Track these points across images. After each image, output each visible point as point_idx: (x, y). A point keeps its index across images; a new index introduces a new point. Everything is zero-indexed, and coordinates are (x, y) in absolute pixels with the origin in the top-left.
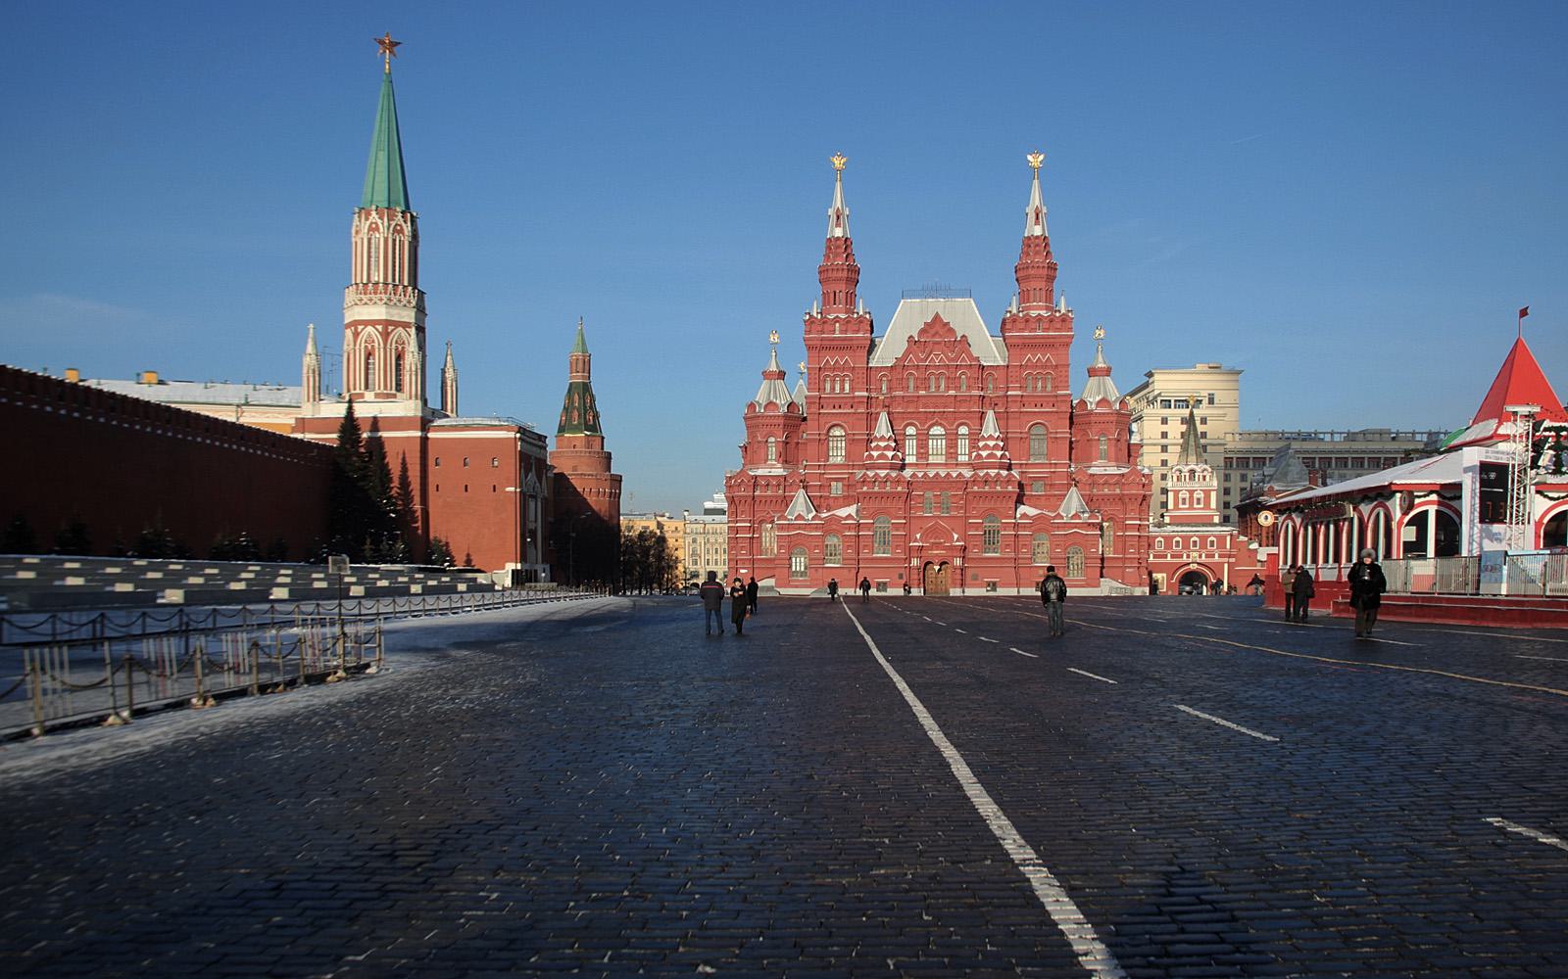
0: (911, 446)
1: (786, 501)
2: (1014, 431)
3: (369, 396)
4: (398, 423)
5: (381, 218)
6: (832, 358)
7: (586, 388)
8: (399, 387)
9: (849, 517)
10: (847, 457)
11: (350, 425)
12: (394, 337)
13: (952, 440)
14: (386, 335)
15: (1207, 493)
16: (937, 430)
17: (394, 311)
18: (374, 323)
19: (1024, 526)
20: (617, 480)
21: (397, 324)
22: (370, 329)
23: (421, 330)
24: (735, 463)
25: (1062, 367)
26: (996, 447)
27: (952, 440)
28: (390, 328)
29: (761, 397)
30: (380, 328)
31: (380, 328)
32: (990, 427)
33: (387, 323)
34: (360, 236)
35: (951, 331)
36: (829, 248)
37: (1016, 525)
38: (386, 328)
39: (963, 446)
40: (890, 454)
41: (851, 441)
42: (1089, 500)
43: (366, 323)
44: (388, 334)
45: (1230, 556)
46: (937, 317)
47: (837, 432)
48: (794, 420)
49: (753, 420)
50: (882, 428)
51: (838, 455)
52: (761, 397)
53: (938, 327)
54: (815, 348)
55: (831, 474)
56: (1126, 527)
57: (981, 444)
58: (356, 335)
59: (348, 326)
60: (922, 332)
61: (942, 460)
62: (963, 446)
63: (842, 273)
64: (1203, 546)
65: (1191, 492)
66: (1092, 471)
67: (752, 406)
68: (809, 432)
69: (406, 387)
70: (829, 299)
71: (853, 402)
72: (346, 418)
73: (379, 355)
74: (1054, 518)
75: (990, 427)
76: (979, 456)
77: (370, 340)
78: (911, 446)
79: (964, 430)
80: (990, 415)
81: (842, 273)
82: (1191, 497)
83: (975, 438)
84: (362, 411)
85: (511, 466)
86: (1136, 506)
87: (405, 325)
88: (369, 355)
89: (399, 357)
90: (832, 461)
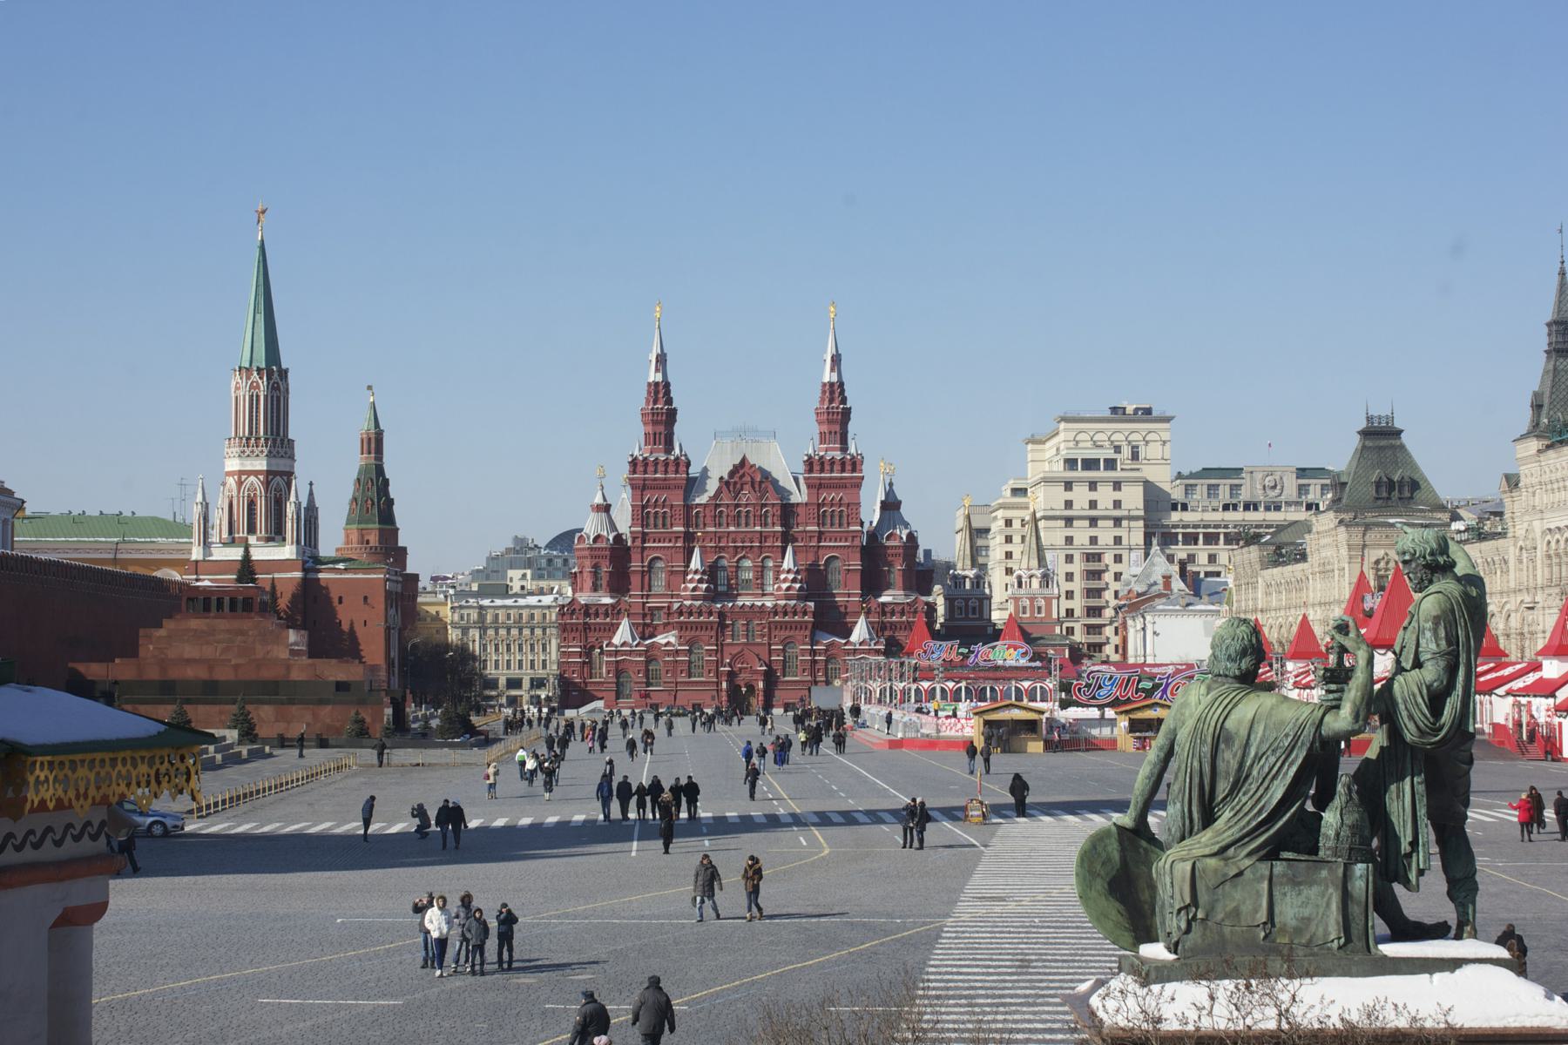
1: (613, 628)
7: (380, 470)
9: (668, 644)
10: (668, 586)
11: (247, 568)
13: (761, 571)
15: (1048, 600)
16: (748, 563)
17: (274, 461)
18: (256, 473)
22: (252, 478)
32: (788, 562)
43: (249, 473)
46: (744, 461)
48: (619, 552)
50: (695, 563)
53: (746, 469)
54: (639, 488)
55: (653, 603)
60: (732, 474)
63: (662, 417)
68: (635, 565)
70: (652, 439)
76: (779, 589)
77: (252, 488)
79: (770, 564)
81: (662, 417)
82: (1032, 605)
85: (379, 602)
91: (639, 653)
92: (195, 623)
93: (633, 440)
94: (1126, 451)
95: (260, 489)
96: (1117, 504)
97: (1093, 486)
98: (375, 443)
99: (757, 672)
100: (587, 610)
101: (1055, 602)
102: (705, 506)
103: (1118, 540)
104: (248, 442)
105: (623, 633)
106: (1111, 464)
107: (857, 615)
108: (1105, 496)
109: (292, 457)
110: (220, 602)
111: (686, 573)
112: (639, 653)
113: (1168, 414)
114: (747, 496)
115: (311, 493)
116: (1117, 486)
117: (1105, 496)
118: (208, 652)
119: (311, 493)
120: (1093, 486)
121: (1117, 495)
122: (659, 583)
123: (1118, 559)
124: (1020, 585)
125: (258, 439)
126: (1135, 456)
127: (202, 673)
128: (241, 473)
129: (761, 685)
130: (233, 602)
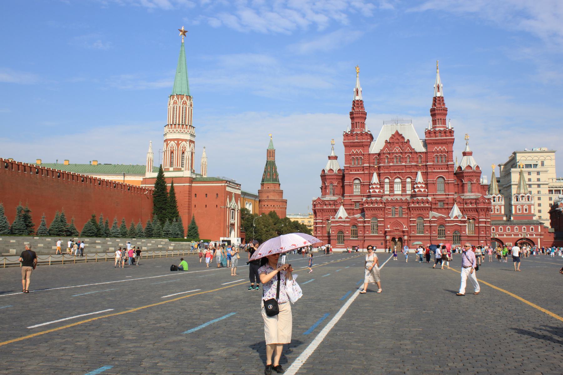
0: (387, 187)
1: (336, 211)
2: (430, 180)
3: (171, 169)
4: (180, 180)
5: (178, 99)
6: (355, 150)
14: (178, 144)
15: (530, 206)
16: (398, 180)
19: (434, 222)
20: (285, 202)
21: (182, 140)
22: (172, 142)
24: (319, 194)
25: (450, 153)
26: (422, 187)
27: (404, 184)
28: (180, 142)
29: (327, 169)
30: (176, 142)
31: (176, 142)
33: (178, 140)
35: (403, 138)
36: (354, 105)
37: (430, 222)
38: (178, 142)
39: (409, 187)
40: (377, 191)
41: (362, 185)
42: (463, 210)
43: (171, 140)
45: (541, 235)
46: (397, 132)
47: (357, 181)
49: (324, 177)
50: (375, 179)
51: (357, 190)
52: (327, 169)
56: (479, 222)
57: (415, 186)
58: (167, 145)
60: (391, 138)
61: (400, 193)
62: (409, 187)
64: (528, 230)
65: (522, 206)
66: (462, 197)
67: (324, 171)
68: (347, 182)
69: (185, 166)
71: (363, 169)
72: (158, 177)
73: (175, 153)
74: (447, 218)
75: (420, 178)
76: (415, 191)
78: (387, 187)
80: (419, 174)
83: (413, 183)
84: (166, 175)
86: (483, 213)
88: (172, 152)
90: (355, 194)
91: (347, 222)
93: (346, 125)
94: (539, 163)
96: (538, 180)
97: (529, 173)
98: (271, 153)
99: (403, 232)
100: (324, 203)
101: (532, 207)
102: (379, 154)
103: (539, 192)
105: (342, 213)
106: (536, 165)
107: (453, 204)
108: (534, 177)
111: (370, 185)
112: (347, 222)
113: (554, 150)
114: (397, 149)
116: (538, 173)
117: (534, 177)
120: (529, 173)
121: (538, 177)
122: (357, 190)
123: (539, 199)
124: (517, 200)
125: (175, 125)
126: (543, 164)
129: (406, 238)
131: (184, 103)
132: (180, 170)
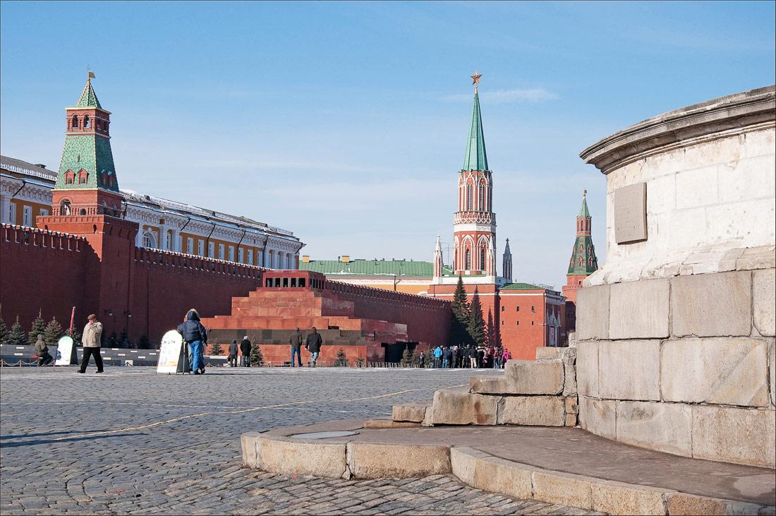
3: (467, 272)
7: (588, 240)
8: (483, 268)
12: (480, 240)
18: (470, 233)
21: (482, 233)
22: (468, 236)
23: (494, 235)
30: (473, 235)
33: (478, 233)
34: (462, 186)
44: (477, 239)
59: (456, 234)
84: (465, 281)
85: (541, 310)
87: (486, 233)
89: (483, 251)
92: (268, 294)
95: (472, 243)
104: (465, 214)
109: (494, 224)
110: (286, 281)
115: (507, 246)
118: (272, 312)
119: (507, 246)
127: (263, 326)
128: (462, 233)
130: (293, 281)
131: (482, 182)
132: (479, 274)
